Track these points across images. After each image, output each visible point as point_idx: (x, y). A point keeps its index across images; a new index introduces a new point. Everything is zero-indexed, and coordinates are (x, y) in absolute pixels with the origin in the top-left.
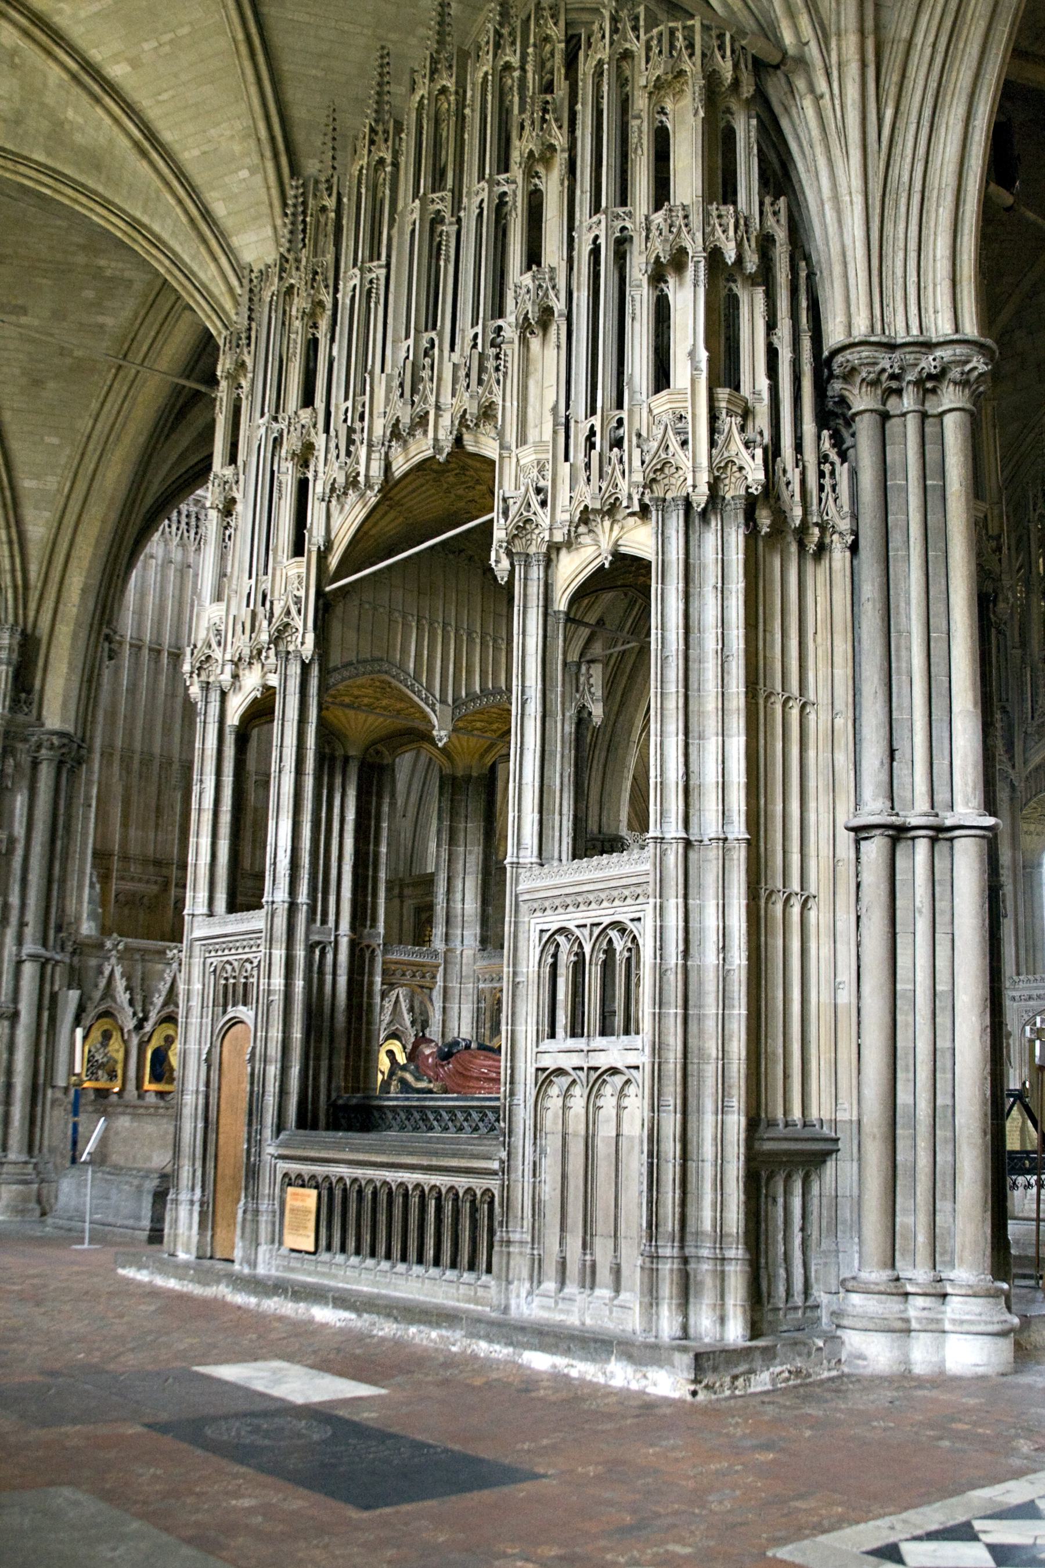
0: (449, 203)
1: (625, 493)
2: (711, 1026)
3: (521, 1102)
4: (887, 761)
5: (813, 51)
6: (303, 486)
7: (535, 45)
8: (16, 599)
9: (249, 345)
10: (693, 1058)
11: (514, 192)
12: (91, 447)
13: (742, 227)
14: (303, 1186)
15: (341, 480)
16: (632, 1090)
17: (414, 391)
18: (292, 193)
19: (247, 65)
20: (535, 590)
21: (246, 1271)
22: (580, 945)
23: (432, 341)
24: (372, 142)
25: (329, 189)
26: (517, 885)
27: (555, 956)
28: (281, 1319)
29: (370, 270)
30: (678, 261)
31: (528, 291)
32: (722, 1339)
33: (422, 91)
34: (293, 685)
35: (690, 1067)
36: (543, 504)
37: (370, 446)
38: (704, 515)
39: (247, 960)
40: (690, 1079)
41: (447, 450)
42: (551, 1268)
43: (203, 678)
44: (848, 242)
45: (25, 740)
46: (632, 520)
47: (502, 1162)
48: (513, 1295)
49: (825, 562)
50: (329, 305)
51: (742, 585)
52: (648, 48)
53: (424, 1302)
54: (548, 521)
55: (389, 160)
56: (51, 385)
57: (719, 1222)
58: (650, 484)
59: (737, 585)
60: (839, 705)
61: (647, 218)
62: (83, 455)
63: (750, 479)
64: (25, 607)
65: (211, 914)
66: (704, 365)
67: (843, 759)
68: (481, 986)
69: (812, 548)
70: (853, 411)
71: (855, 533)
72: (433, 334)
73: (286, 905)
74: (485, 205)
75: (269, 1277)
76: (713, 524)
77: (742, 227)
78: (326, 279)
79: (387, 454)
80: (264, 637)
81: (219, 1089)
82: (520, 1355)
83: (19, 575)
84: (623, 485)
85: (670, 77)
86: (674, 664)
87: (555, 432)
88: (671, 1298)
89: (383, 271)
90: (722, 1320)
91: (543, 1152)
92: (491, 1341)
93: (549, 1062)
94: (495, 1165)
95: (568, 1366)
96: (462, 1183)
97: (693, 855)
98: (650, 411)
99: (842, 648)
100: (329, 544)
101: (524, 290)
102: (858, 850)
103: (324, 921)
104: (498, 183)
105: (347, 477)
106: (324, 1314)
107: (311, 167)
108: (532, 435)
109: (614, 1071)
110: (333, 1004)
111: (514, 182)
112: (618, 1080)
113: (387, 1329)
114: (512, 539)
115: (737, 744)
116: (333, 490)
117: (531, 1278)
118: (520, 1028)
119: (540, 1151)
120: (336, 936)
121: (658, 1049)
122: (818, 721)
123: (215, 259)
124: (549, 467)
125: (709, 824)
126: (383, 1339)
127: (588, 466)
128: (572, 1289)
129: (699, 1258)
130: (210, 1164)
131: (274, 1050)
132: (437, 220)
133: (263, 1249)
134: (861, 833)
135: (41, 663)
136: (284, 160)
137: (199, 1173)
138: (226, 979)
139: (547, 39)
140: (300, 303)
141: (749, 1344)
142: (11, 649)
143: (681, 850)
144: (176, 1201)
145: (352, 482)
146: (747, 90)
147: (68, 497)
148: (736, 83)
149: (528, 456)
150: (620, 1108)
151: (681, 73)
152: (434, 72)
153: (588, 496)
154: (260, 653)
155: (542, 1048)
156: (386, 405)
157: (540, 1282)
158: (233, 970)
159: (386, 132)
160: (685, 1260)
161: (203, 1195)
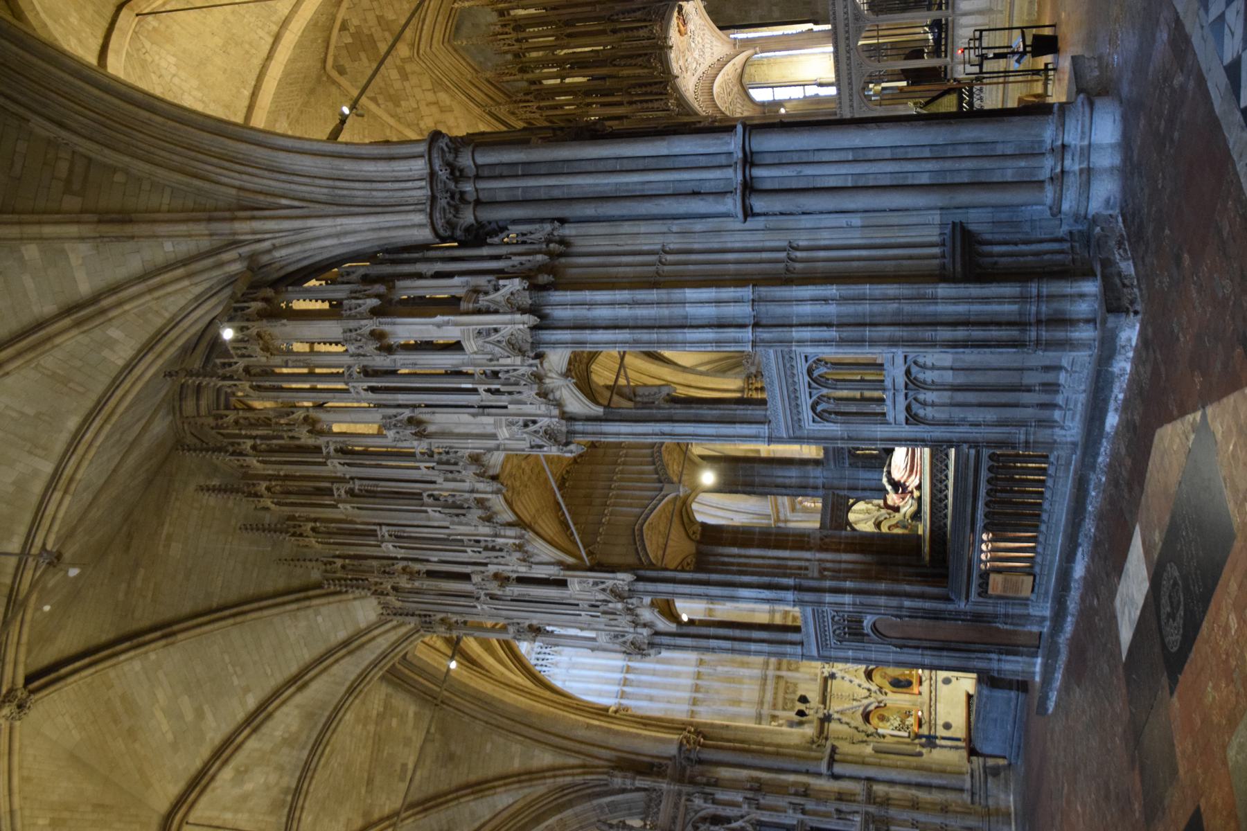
0: (341, 485)
1: (528, 368)
2: (877, 308)
3: (929, 435)
4: (700, 197)
5: (245, 250)
6: (522, 580)
7: (240, 429)
8: (592, 773)
9: (430, 616)
10: (899, 319)
11: (335, 442)
12: (493, 722)
13: (357, 295)
15: (519, 555)
16: (921, 360)
17: (461, 507)
18: (332, 587)
19: (249, 616)
20: (590, 427)
21: (1048, 623)
22: (822, 396)
23: (430, 496)
24: (301, 535)
25: (330, 563)
26: (782, 438)
27: (830, 413)
28: (1083, 599)
29: (383, 536)
30: (377, 336)
31: (398, 433)
32: (1095, 296)
33: (268, 503)
34: (650, 587)
35: (905, 321)
36: (534, 422)
37: (496, 536)
38: (543, 317)
40: (913, 321)
41: (499, 486)
42: (1044, 414)
43: (645, 647)
44: (365, 227)
45: (684, 769)
46: (546, 365)
47: (970, 447)
48: (1064, 439)
49: (572, 240)
50: (404, 563)
51: (587, 293)
52: (243, 356)
53: (1070, 501)
54: (546, 419)
55: (313, 524)
56: (453, 747)
57: (1012, 300)
58: (522, 352)
59: (587, 295)
60: (664, 229)
61: (352, 356)
62: (499, 727)
63: (519, 288)
64: (598, 767)
65: (802, 643)
66: (446, 318)
67: (699, 226)
68: (847, 465)
69: (562, 248)
70: (474, 222)
71: (552, 220)
72: (425, 495)
74: (342, 461)
75: (1052, 608)
76: (548, 311)
77: (357, 295)
78: (389, 566)
79: (501, 525)
80: (620, 606)
81: (920, 639)
82: (1108, 433)
83: (576, 771)
84: (523, 370)
85: (261, 342)
86: (639, 336)
87: (488, 415)
88: (1067, 331)
89: (385, 529)
90: (1082, 296)
91: (963, 420)
92: (1098, 454)
93: (902, 416)
94: (973, 451)
95: (1116, 400)
96: (984, 475)
97: (764, 322)
98: (475, 353)
99: (627, 228)
100: (560, 563)
101: (397, 436)
102: (759, 215)
103: (806, 569)
104: (328, 453)
105: (516, 551)
106: (1079, 570)
107: (316, 575)
108: (490, 430)
109: (908, 373)
110: (861, 563)
111: (328, 443)
112: (914, 369)
113: (1089, 527)
114: (557, 442)
115: (691, 294)
116: (524, 560)
117: (1052, 427)
118: (879, 435)
119: (962, 422)
120: (815, 560)
121: (893, 343)
122: (674, 243)
123: (374, 638)
124: (510, 418)
125: (743, 311)
126: (1097, 528)
127: (510, 393)
128: (1060, 399)
129: (1038, 313)
130: (973, 647)
131: (894, 602)
132: (351, 493)
133: (1031, 611)
134: (748, 213)
135: (634, 757)
136: (311, 593)
137: (979, 655)
138: (845, 634)
139: (236, 422)
140: (404, 582)
141: (1099, 277)
142: (625, 777)
143: (761, 330)
144: (999, 671)
145: (519, 548)
146: (269, 292)
147: (526, 737)
148: (265, 300)
149: (504, 433)
150: (933, 368)
151: (259, 335)
152: (256, 495)
153: (529, 393)
154: (629, 609)
155: (892, 420)
156: (470, 525)
157: (1056, 422)
158: (839, 629)
159: (294, 527)
160: (1039, 322)
161: (995, 652)
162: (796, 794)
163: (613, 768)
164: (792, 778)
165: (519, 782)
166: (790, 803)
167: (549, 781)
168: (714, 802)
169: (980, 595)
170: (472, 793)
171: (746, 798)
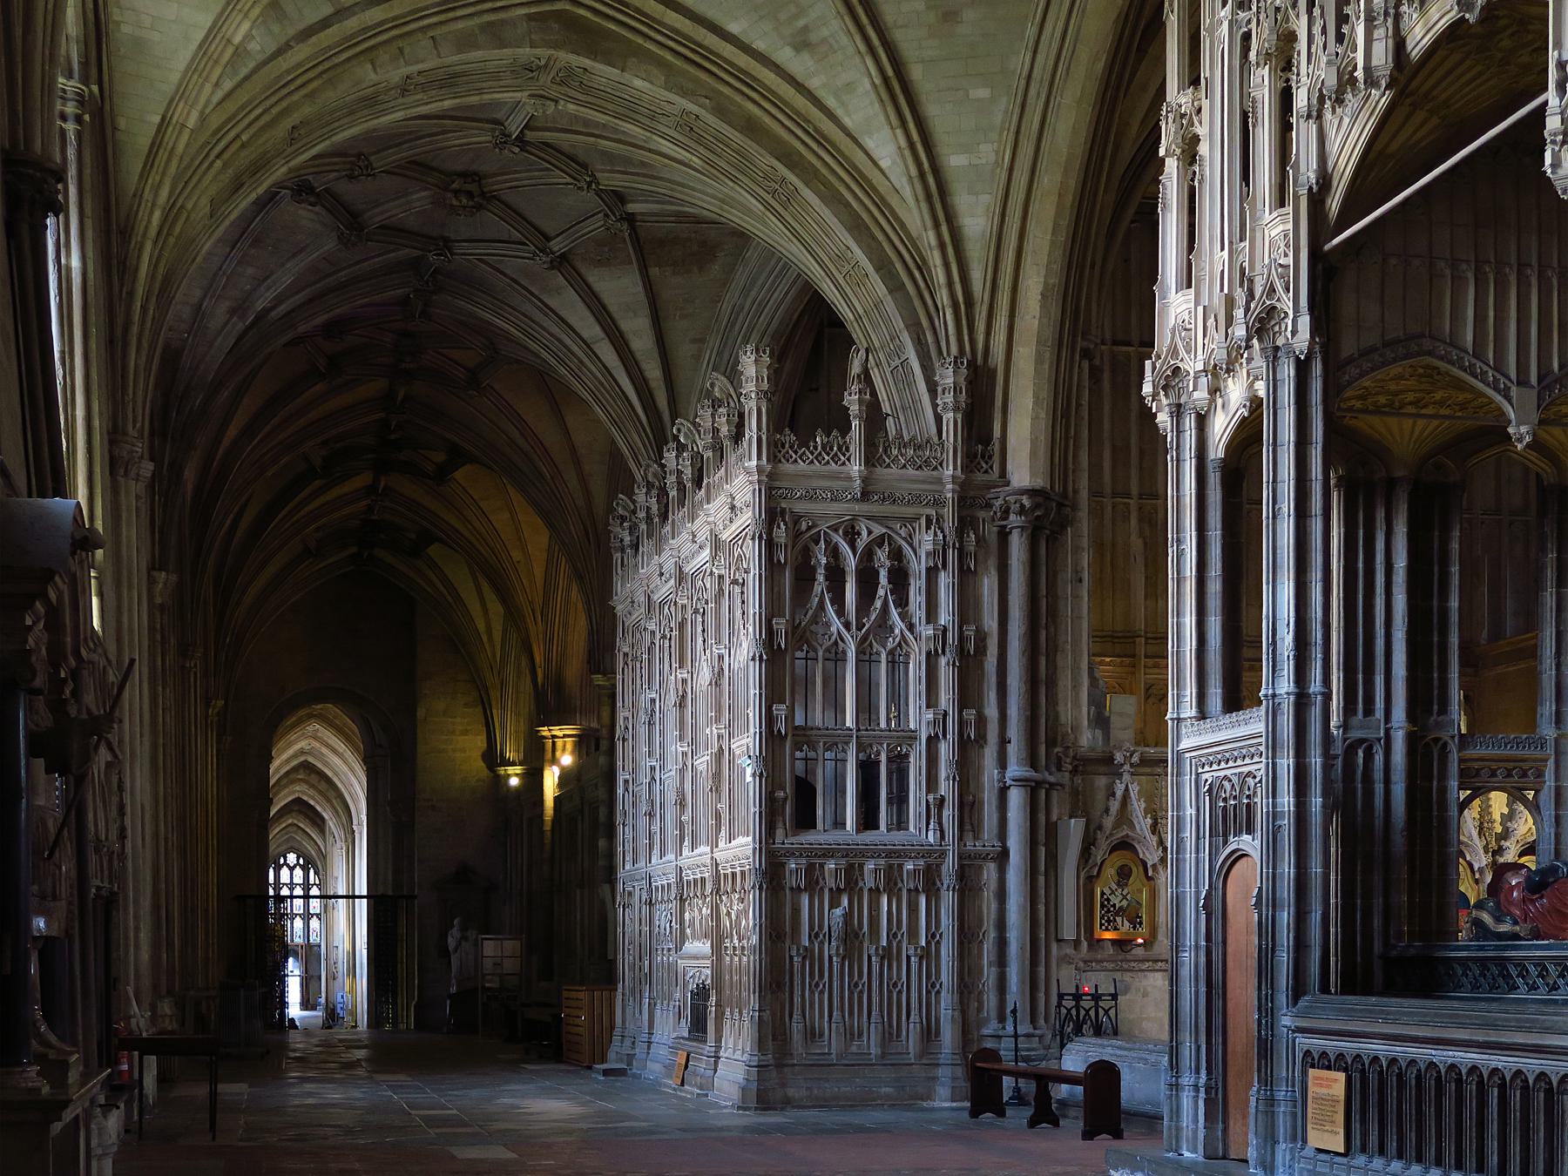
14: (1329, 1068)
39: (1249, 774)
73: (1292, 698)
162: (962, 724)
163: (972, 364)
164: (992, 711)
165: (922, 175)
166: (945, 714)
167: (931, 236)
168: (932, 573)
169: (1308, 1053)
170: (886, 80)
171: (945, 630)
